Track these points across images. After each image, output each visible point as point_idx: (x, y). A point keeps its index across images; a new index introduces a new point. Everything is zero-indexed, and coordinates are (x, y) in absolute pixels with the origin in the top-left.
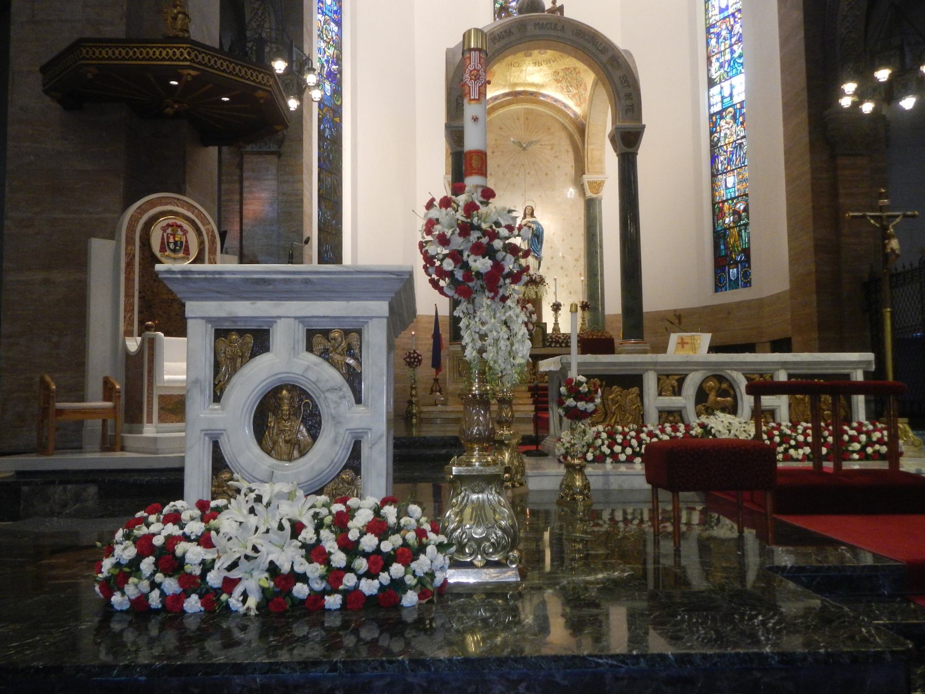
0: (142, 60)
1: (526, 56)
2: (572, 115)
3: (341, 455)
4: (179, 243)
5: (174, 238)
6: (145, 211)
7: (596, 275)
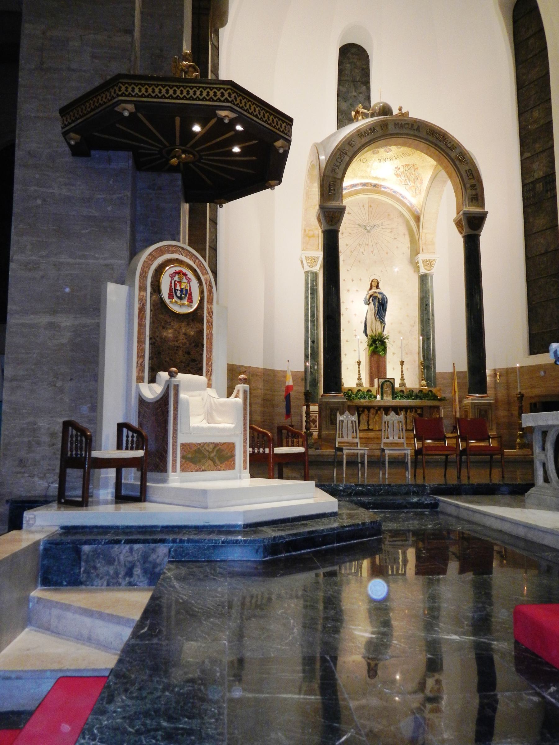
0: (182, 99)
1: (374, 153)
2: (408, 204)
4: (184, 290)
5: (180, 286)
6: (155, 258)
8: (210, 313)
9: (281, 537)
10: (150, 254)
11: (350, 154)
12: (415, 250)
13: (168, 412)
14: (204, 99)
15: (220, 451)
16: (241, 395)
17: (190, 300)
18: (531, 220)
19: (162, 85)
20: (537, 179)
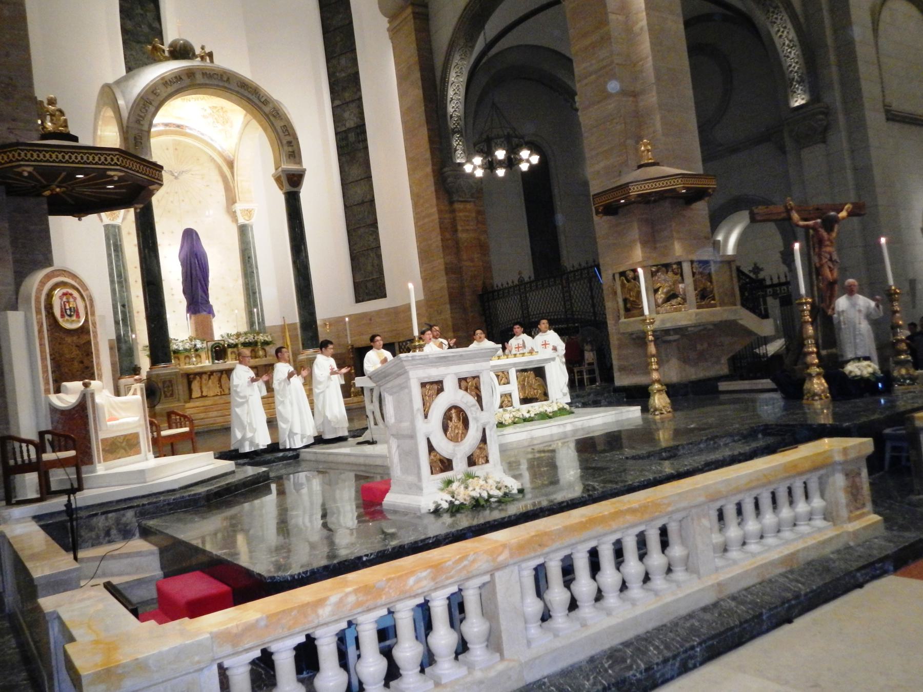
2: (220, 149)
3: (479, 436)
7: (254, 293)
8: (94, 324)
9: (211, 490)
10: (41, 282)
11: (155, 104)
12: (231, 199)
13: (87, 416)
14: (96, 163)
15: (128, 440)
16: (139, 392)
17: (78, 316)
18: (347, 169)
19: (57, 151)
20: (349, 130)
